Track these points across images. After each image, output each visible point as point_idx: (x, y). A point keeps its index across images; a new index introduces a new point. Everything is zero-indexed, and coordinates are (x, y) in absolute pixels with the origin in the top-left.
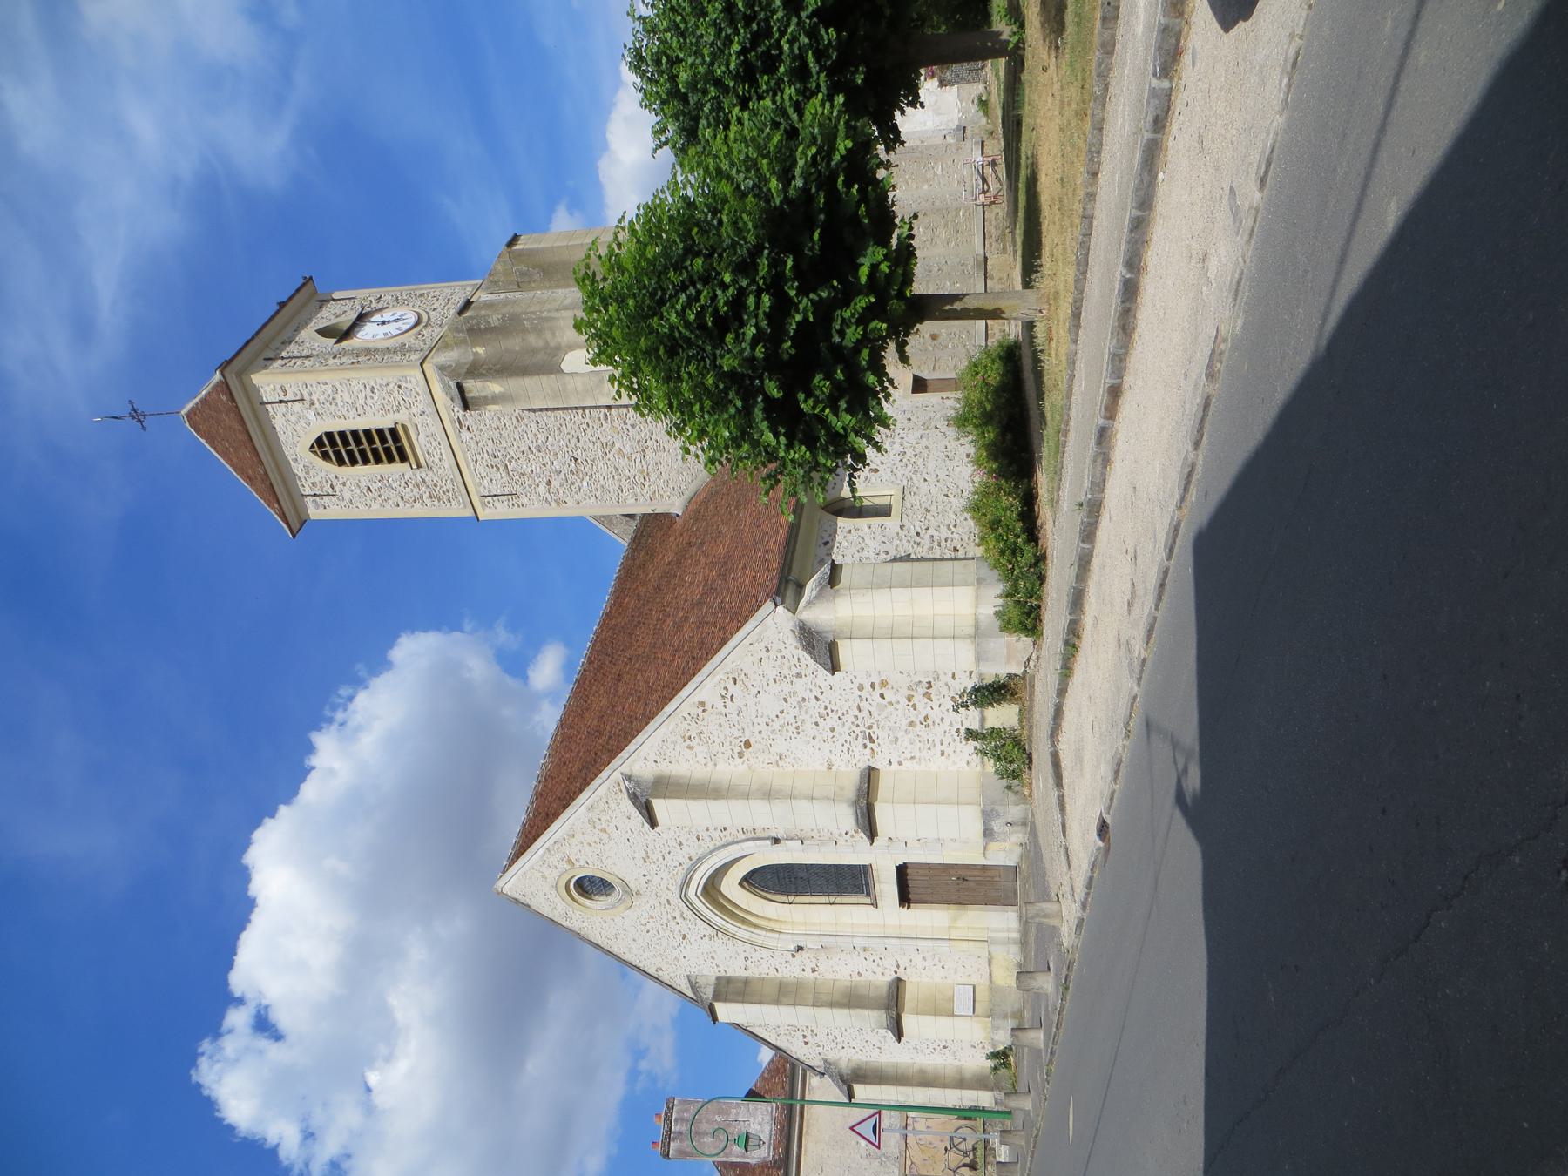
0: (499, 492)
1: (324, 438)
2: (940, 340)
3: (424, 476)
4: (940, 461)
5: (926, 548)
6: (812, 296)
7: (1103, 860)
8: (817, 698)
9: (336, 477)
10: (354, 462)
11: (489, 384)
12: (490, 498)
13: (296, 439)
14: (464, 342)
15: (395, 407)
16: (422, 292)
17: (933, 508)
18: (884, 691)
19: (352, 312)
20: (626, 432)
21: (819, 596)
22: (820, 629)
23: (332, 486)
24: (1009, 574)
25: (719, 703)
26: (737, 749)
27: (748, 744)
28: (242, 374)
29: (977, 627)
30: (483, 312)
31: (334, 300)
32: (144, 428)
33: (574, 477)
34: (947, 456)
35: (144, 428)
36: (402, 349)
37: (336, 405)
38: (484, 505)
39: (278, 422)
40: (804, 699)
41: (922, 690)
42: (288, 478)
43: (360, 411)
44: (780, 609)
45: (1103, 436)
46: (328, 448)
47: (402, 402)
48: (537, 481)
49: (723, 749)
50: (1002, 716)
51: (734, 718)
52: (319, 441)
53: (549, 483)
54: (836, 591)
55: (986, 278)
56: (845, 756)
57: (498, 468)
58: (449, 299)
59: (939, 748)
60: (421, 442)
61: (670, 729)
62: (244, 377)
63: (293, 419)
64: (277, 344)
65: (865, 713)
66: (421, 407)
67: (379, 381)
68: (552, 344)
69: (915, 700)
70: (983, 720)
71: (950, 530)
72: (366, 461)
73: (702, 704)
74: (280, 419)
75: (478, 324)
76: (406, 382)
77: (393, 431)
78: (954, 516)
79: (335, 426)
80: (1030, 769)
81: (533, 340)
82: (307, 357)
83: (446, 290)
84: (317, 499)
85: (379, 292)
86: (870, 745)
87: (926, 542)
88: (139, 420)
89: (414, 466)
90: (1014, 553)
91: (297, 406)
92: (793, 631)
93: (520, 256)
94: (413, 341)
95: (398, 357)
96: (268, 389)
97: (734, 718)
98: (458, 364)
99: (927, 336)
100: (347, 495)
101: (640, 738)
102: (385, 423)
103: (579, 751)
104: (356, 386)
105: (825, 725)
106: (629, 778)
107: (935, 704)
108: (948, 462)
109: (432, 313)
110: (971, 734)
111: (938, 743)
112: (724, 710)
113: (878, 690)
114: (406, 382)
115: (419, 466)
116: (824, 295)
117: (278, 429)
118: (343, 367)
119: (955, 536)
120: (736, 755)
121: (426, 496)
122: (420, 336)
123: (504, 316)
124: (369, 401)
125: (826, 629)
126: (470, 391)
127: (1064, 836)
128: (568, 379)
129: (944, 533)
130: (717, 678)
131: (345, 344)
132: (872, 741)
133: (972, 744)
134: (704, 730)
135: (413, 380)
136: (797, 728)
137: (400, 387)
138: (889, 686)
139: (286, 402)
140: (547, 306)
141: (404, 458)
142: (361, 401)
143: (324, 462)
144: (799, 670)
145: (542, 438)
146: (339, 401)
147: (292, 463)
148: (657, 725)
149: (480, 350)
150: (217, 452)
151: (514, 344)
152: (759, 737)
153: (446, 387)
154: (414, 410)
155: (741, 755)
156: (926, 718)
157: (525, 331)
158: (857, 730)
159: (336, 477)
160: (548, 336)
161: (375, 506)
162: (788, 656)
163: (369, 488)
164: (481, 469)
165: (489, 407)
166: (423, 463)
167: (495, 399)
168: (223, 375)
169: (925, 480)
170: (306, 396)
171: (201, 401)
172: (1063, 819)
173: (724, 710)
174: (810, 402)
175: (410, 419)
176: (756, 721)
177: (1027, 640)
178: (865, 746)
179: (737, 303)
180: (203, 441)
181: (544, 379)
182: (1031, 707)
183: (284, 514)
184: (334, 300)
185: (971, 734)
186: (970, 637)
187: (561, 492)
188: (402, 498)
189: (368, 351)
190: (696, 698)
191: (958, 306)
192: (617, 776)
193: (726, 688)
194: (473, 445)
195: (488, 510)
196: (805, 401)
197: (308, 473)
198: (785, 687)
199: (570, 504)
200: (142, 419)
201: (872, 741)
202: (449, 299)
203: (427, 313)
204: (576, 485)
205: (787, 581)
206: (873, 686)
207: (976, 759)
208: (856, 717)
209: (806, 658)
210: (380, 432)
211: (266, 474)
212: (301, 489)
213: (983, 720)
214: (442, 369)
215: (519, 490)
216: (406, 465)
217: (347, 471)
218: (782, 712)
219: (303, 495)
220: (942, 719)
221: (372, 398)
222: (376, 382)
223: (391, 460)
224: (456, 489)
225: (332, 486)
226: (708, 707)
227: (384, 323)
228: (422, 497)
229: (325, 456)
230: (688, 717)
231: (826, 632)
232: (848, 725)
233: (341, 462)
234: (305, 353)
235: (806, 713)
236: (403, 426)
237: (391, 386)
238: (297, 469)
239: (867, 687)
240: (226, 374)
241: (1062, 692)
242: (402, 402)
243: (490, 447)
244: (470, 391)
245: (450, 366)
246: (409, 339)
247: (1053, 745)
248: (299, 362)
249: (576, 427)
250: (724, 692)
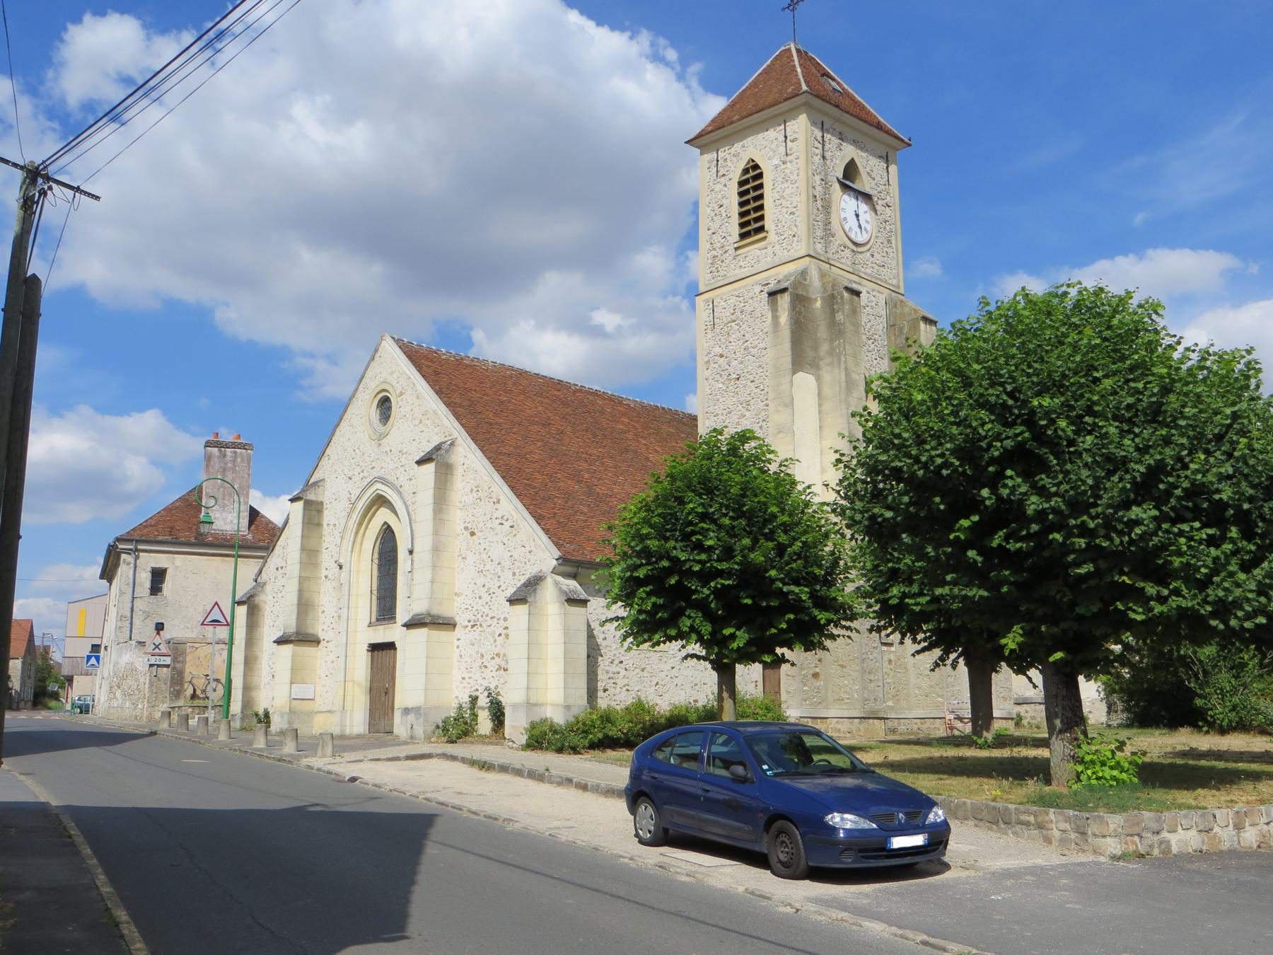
0: (715, 314)
1: (759, 171)
2: (812, 680)
3: (730, 252)
4: (692, 679)
5: (608, 668)
6: (712, 597)
7: (339, 780)
8: (499, 587)
9: (730, 179)
10: (741, 194)
11: (787, 313)
12: (711, 306)
13: (759, 148)
14: (825, 290)
15: (779, 231)
16: (894, 242)
17: (645, 674)
18: (503, 636)
19: (873, 185)
20: (757, 421)
21: (561, 591)
22: (538, 592)
23: (724, 175)
24: (571, 728)
25: (498, 514)
26: (469, 526)
27: (473, 534)
28: (807, 107)
29: (535, 705)
30: (847, 307)
31: (887, 167)
32: (783, 9)
33: (726, 377)
34: (696, 685)
35: (783, 9)
36: (828, 234)
37: (782, 183)
38: (707, 301)
39: (771, 134)
40: (499, 577)
41: (503, 664)
42: (731, 139)
43: (778, 202)
44: (555, 562)
45: (453, 758)
46: (752, 173)
47: (783, 237)
48: (723, 346)
49: (470, 515)
50: (485, 724)
51: (489, 525)
52: (756, 167)
53: (721, 356)
54: (563, 603)
55: (861, 718)
56: (464, 607)
57: (733, 314)
58: (884, 266)
59: (467, 676)
60: (755, 252)
61: (484, 477)
62: (804, 108)
63: (773, 146)
64: (839, 127)
65: (489, 622)
66: (779, 253)
67: (798, 219)
68: (821, 363)
69: (497, 659)
70: (483, 708)
71: (624, 686)
72: (741, 204)
73: (498, 502)
74: (774, 134)
75: (837, 303)
76: (798, 242)
77: (761, 229)
78: (637, 689)
79: (767, 181)
80: (447, 742)
81: (825, 347)
82: (824, 157)
83: (894, 263)
84: (715, 162)
85: (894, 204)
86: (470, 624)
87: (613, 668)
88: (790, 5)
89: (736, 245)
90: (583, 732)
91: (782, 150)
92: (541, 571)
93: (915, 327)
94: (837, 244)
95: (819, 233)
96: (795, 127)
97: (489, 525)
98: (806, 287)
99: (817, 670)
100: (718, 187)
101: (479, 453)
102: (768, 223)
103: (488, 396)
104: (795, 199)
105: (483, 592)
106: (452, 444)
107: (494, 674)
108: (691, 685)
109: (869, 254)
110: (474, 700)
111: (470, 675)
112: (494, 518)
113: (503, 632)
114: (798, 242)
115: (736, 249)
116: (713, 605)
117: (766, 133)
118: (810, 188)
119: (618, 690)
120: (466, 525)
121: (715, 253)
122: (842, 248)
123: (843, 324)
124: (784, 210)
125: (538, 597)
126: (782, 298)
127: (371, 760)
128: (787, 379)
129: (621, 682)
130: (514, 514)
131: (837, 186)
132: (473, 626)
133: (467, 699)
134: (483, 502)
135: (799, 247)
136: (482, 571)
137: (794, 236)
138: (506, 640)
139: (785, 141)
140: (850, 359)
141: (743, 236)
142: (784, 203)
143: (741, 170)
144: (517, 574)
145: (754, 351)
146: (786, 185)
147: (741, 143)
148: (486, 467)
149: (818, 304)
150: (758, 75)
151: (822, 332)
152: (477, 543)
153: (786, 278)
154: (777, 247)
155: (466, 528)
156: (486, 667)
157: (832, 341)
158: (479, 616)
159: (730, 179)
160: (828, 360)
161: (709, 210)
162: (526, 567)
163: (721, 206)
164: (732, 301)
165: (770, 312)
166: (740, 252)
167: (775, 318)
168: (804, 92)
169: (673, 668)
170: (789, 158)
171: (794, 66)
172: (382, 760)
173: (494, 518)
174: (644, 595)
175: (770, 243)
176: (487, 540)
177: (523, 739)
178: (469, 621)
179: (699, 547)
180: (769, 62)
181: (789, 359)
182: (484, 743)
183: (703, 136)
184: (887, 167)
185: (474, 700)
186: (528, 700)
187: (715, 365)
188: (714, 233)
189: (827, 208)
190: (502, 498)
191: (725, 695)
192: (456, 434)
193: (507, 520)
194: (751, 294)
195: (702, 304)
196: (644, 591)
197: (734, 155)
198: (507, 564)
199: (706, 372)
200: (791, 8)
201: (473, 626)
202: (884, 266)
203: (868, 250)
204: (720, 379)
205: (578, 567)
206: (506, 628)
207: (455, 704)
208: (487, 615)
209: (523, 579)
210: (761, 218)
211: (732, 123)
212: (723, 150)
213: (483, 708)
214: (804, 273)
215: (717, 331)
216: (737, 238)
217: (734, 189)
218: (492, 561)
219: (718, 150)
220: (485, 678)
221: (787, 213)
222: (797, 216)
223: (742, 225)
224: (719, 278)
225: (724, 175)
226: (497, 506)
227: (857, 216)
228: (714, 249)
229: (746, 171)
230: (491, 490)
231: (535, 596)
232: (483, 609)
233: (741, 184)
234: (828, 154)
235: (491, 579)
236: (766, 237)
237: (795, 229)
238: (737, 147)
239: (505, 624)
240: (805, 95)
241: (464, 760)
242: (783, 237)
243: (748, 309)
244: (782, 298)
245: (805, 280)
246: (840, 238)
247: (437, 755)
248: (819, 151)
249: (762, 380)
250: (505, 518)
